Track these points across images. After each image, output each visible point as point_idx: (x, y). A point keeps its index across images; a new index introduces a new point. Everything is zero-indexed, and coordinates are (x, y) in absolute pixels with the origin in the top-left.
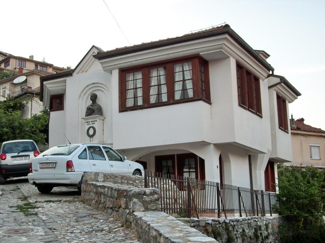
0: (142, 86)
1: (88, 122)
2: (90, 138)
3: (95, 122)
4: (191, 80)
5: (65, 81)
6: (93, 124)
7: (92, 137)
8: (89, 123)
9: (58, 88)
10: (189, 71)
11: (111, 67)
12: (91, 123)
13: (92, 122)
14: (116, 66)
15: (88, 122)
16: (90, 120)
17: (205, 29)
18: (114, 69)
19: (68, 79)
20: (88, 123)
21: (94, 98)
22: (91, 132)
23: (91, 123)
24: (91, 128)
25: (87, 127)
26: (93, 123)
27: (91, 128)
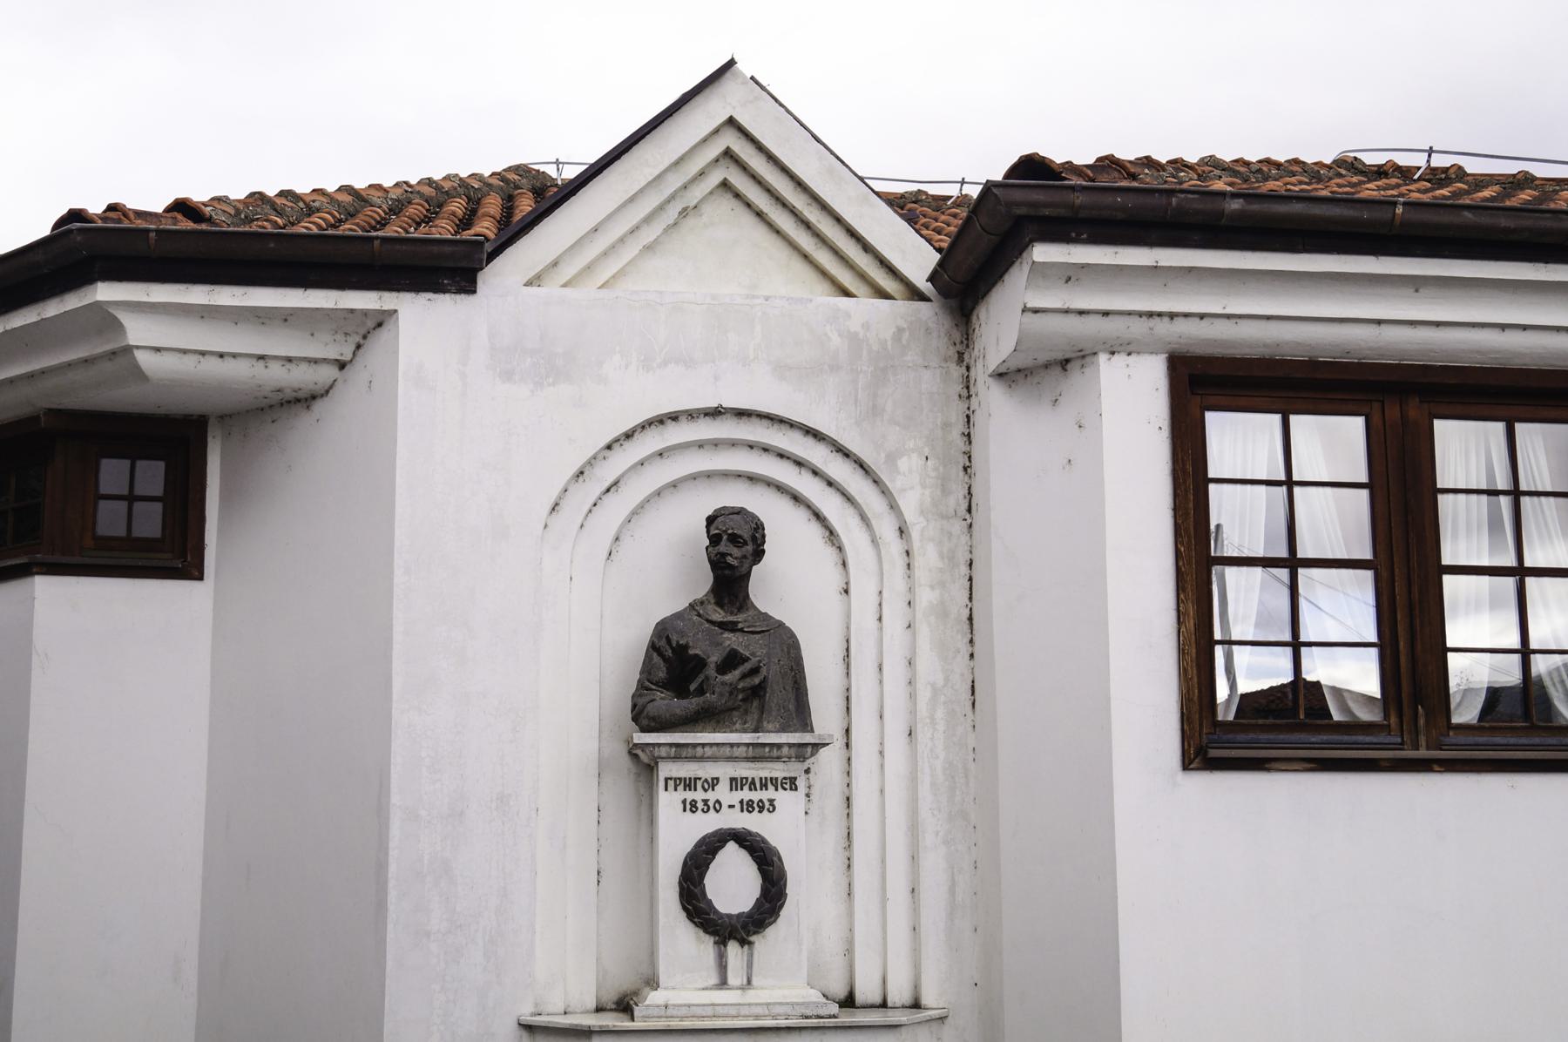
0: (1367, 555)
1: (689, 784)
2: (722, 942)
3: (770, 793)
4: (1230, 551)
5: (381, 320)
6: (748, 806)
7: (743, 942)
8: (711, 796)
9: (212, 367)
10: (1484, 498)
11: (1093, 326)
12: (722, 792)
13: (736, 784)
14: (1163, 328)
15: (689, 784)
16: (724, 771)
17: (914, 187)
18: (1126, 347)
19: (420, 318)
20: (699, 795)
21: (733, 548)
22: (733, 883)
23: (722, 792)
24: (732, 846)
25: (679, 831)
26: (746, 794)
27: (732, 846)
